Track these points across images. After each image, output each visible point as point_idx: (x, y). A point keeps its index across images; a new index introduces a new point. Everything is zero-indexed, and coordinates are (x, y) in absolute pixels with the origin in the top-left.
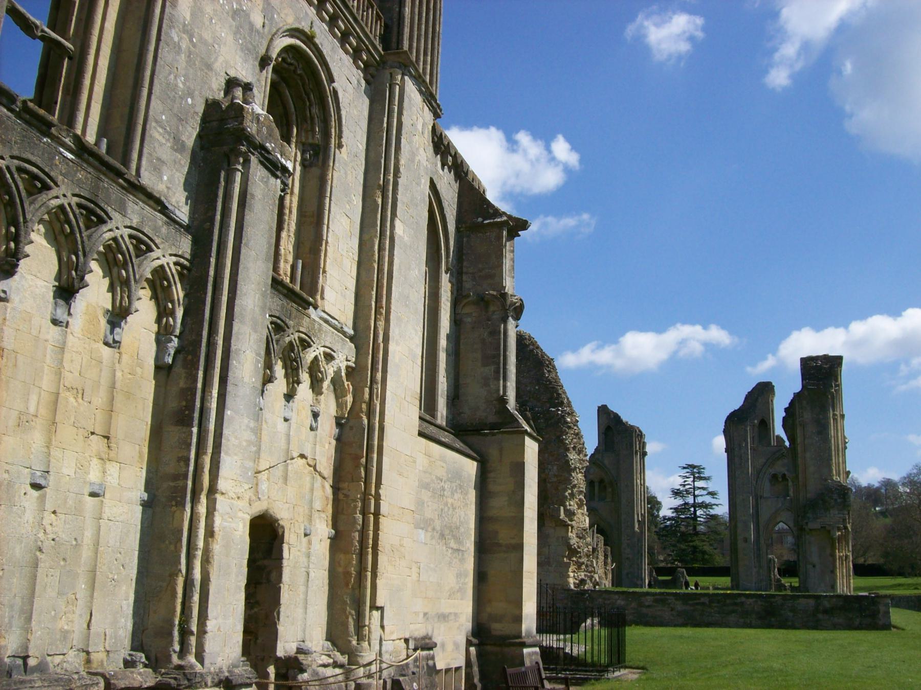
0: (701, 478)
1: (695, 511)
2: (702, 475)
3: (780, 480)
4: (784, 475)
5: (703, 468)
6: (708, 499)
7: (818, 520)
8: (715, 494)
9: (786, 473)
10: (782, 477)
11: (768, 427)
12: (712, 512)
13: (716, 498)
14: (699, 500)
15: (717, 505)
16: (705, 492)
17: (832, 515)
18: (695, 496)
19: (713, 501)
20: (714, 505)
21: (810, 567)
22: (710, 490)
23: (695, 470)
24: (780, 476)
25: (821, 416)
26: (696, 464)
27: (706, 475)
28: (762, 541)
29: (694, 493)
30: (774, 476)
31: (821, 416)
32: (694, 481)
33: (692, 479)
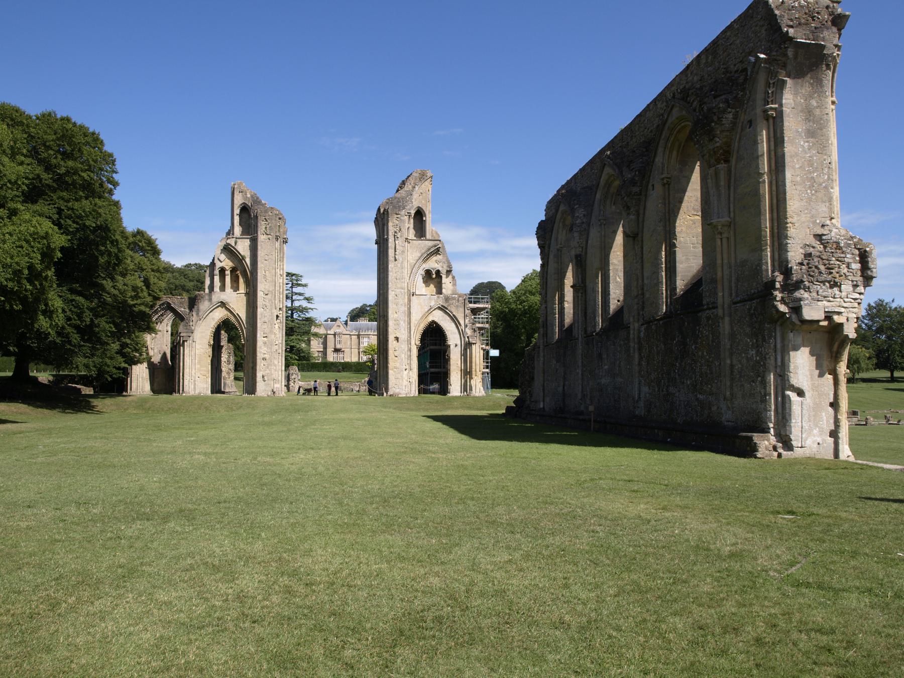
0: (299, 285)
1: (292, 314)
2: (299, 282)
3: (434, 276)
4: (438, 272)
5: (301, 276)
6: (305, 304)
7: (820, 303)
8: (311, 299)
9: (440, 269)
10: (436, 273)
11: (424, 219)
12: (308, 315)
13: (311, 303)
14: (296, 304)
15: (312, 309)
16: (301, 298)
17: (844, 294)
18: (292, 301)
19: (309, 306)
20: (310, 309)
21: (793, 395)
22: (307, 296)
23: (293, 278)
24: (434, 273)
25: (814, 103)
26: (294, 272)
27: (303, 282)
28: (413, 343)
29: (292, 298)
30: (428, 273)
31: (814, 103)
32: (292, 287)
33: (290, 285)
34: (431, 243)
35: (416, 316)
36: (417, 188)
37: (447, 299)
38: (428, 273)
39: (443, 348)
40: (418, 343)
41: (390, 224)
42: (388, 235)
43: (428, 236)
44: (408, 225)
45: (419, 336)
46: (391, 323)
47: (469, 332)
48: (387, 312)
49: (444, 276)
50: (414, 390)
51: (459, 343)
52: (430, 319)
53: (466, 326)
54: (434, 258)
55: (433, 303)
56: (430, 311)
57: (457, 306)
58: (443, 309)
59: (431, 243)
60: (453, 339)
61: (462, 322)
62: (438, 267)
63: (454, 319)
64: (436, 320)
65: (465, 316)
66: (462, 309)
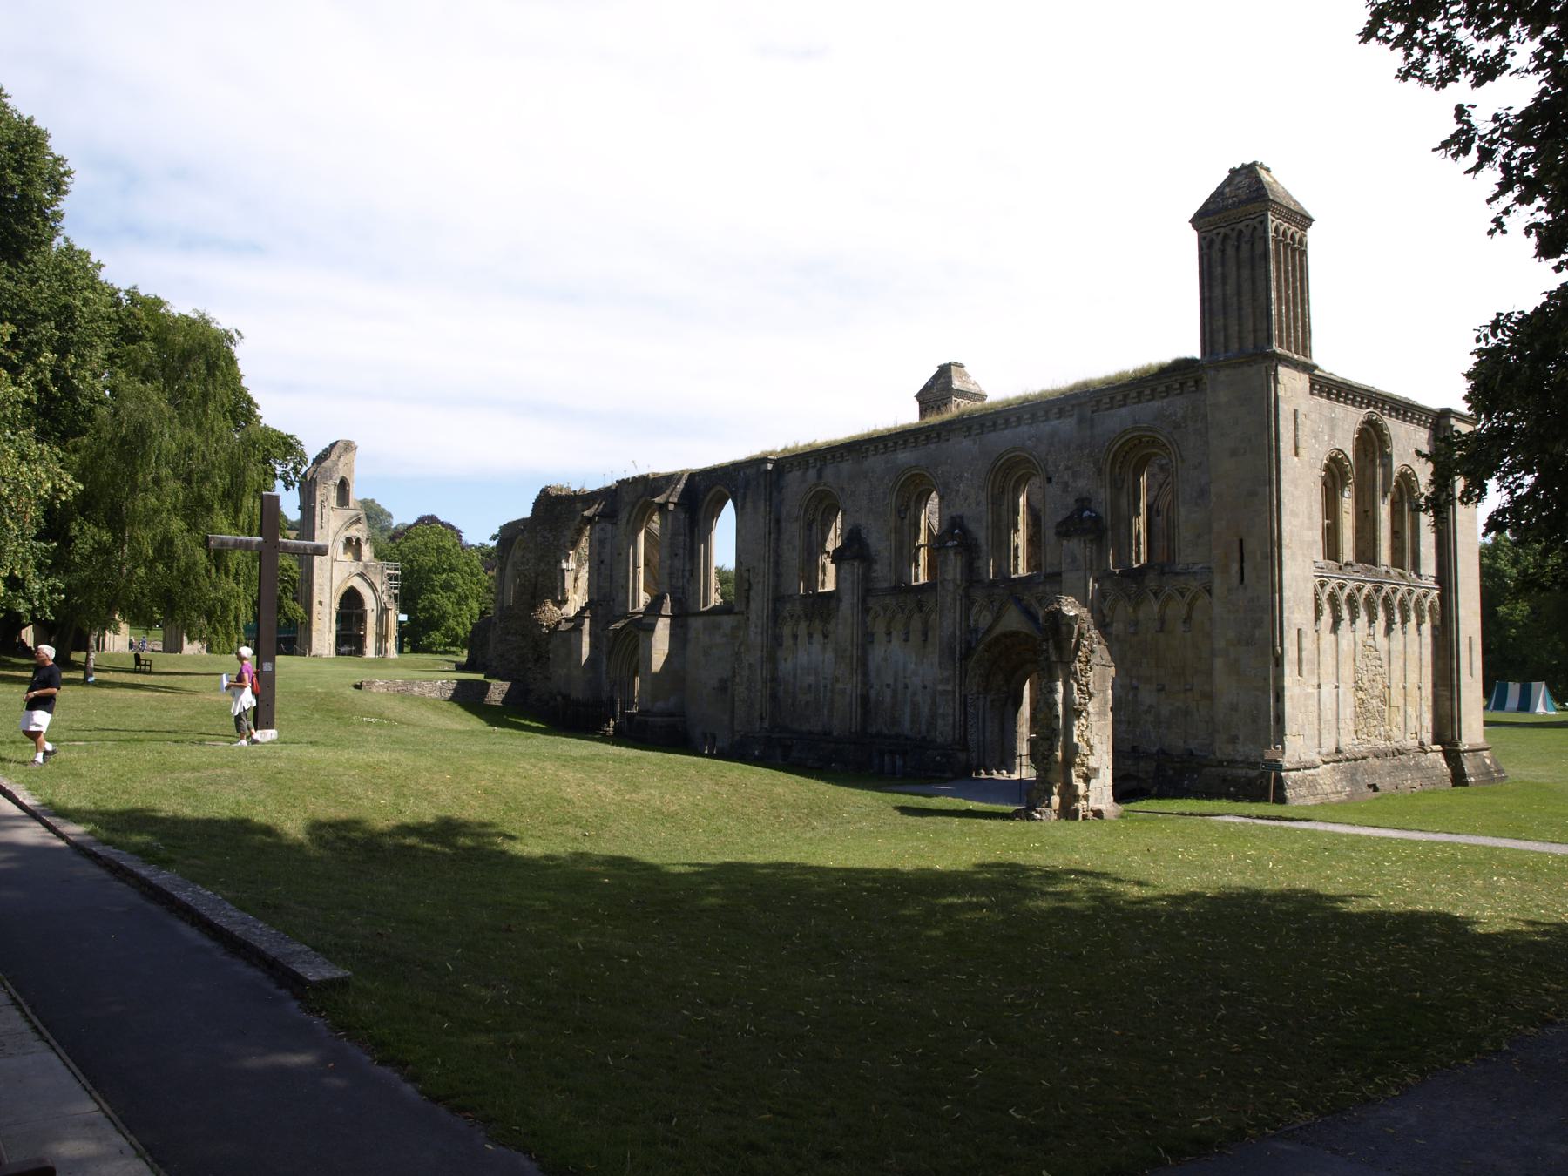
30: (349, 540)
34: (354, 513)
35: (336, 582)
36: (342, 458)
37: (366, 566)
38: (349, 540)
39: (359, 611)
40: (337, 607)
41: (318, 493)
42: (315, 503)
43: (351, 506)
44: (333, 494)
45: (338, 601)
46: (316, 588)
47: (385, 598)
48: (312, 578)
49: (363, 544)
50: (333, 654)
51: (375, 608)
52: (349, 584)
53: (382, 593)
54: (355, 527)
55: (352, 570)
56: (350, 576)
57: (375, 574)
58: (361, 575)
59: (354, 513)
60: (370, 604)
61: (379, 589)
62: (359, 535)
63: (372, 585)
64: (355, 585)
65: (382, 583)
66: (379, 576)
